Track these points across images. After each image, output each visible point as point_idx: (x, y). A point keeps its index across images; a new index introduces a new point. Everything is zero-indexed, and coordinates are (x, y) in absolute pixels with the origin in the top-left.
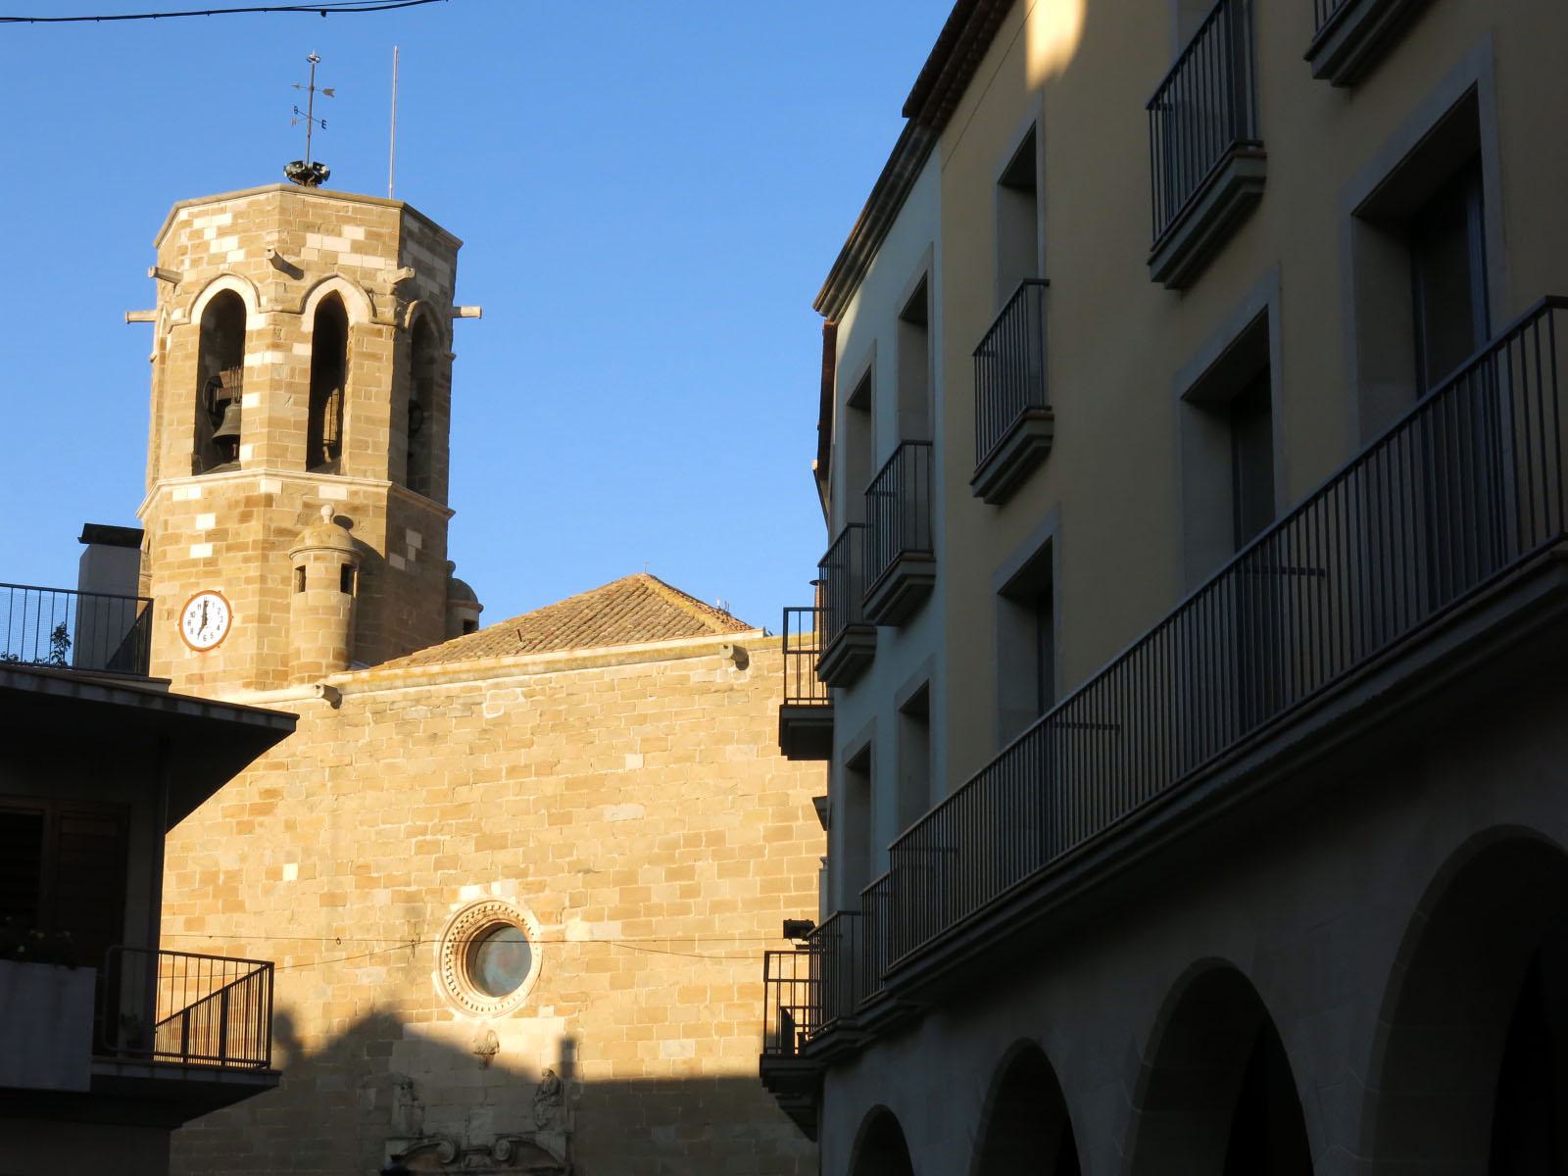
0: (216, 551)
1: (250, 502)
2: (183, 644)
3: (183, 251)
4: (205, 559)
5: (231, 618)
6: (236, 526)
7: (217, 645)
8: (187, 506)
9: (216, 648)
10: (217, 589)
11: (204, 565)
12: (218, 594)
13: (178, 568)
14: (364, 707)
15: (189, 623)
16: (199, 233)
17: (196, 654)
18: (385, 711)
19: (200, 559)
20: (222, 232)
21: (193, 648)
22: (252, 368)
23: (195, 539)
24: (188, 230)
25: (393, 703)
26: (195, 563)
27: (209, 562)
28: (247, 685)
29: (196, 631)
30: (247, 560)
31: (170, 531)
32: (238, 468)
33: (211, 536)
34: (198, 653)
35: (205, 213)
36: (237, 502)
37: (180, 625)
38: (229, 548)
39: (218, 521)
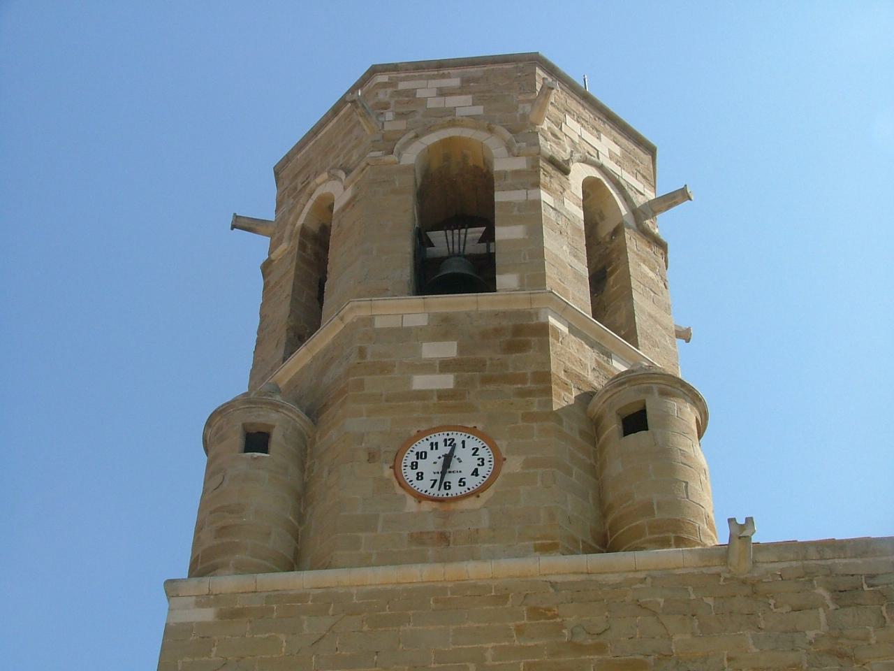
0: (457, 383)
1: (518, 330)
2: (400, 491)
3: (386, 106)
4: (438, 391)
5: (499, 461)
6: (500, 356)
7: (476, 493)
8: (404, 335)
9: (473, 498)
10: (471, 425)
11: (440, 397)
12: (473, 431)
13: (387, 401)
14: (811, 581)
15: (414, 466)
16: (411, 93)
17: (426, 506)
18: (858, 588)
19: (432, 391)
20: (442, 93)
21: (420, 497)
22: (508, 204)
23: (427, 367)
24: (389, 90)
25: (873, 576)
26: (422, 395)
27: (442, 395)
28: (547, 548)
29: (429, 476)
30: (522, 394)
31: (369, 359)
32: (495, 290)
33: (446, 366)
34: (435, 505)
35: (421, 78)
36: (498, 331)
37: (396, 468)
38: (486, 380)
39: (461, 349)
